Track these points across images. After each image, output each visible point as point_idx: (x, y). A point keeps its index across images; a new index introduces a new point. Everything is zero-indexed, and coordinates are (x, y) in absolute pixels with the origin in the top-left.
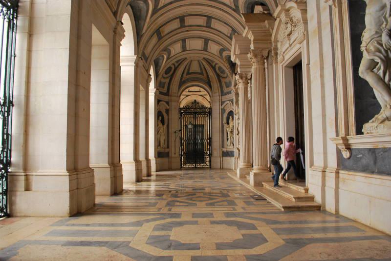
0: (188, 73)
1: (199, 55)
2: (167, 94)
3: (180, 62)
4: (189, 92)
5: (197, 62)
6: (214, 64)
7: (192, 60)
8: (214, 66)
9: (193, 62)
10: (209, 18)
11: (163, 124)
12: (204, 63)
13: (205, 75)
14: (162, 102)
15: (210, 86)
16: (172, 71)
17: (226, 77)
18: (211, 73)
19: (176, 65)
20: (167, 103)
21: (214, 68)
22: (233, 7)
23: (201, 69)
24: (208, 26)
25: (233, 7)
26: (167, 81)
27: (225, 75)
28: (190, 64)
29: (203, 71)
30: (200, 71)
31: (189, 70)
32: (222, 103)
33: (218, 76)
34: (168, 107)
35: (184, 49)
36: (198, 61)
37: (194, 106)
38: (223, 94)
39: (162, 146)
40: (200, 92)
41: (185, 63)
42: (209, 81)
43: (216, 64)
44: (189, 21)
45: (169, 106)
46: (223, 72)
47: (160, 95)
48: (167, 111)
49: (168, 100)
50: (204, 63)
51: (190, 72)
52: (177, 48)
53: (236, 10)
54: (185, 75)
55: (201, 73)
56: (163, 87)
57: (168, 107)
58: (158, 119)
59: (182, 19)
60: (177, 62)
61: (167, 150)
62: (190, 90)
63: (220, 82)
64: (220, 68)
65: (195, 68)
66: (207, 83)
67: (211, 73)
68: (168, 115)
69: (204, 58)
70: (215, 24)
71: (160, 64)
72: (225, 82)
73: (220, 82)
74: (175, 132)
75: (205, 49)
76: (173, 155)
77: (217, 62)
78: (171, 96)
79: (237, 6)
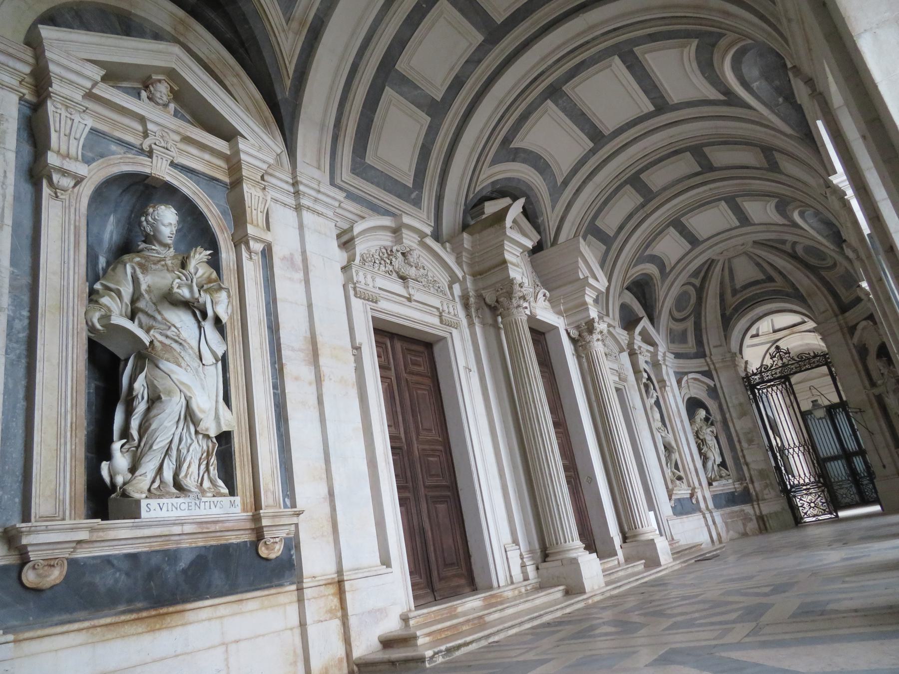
1: (740, 240)
2: (701, 354)
3: (704, 272)
4: (775, 331)
6: (788, 247)
7: (729, 260)
8: (790, 251)
10: (697, 151)
12: (763, 254)
14: (691, 376)
16: (693, 300)
17: (835, 265)
19: (697, 282)
20: (708, 374)
22: (722, 97)
24: (707, 167)
25: (722, 97)
26: (690, 324)
27: (830, 262)
28: (731, 271)
30: (761, 277)
32: (852, 329)
34: (711, 383)
35: (693, 241)
36: (747, 254)
37: (780, 362)
38: (844, 308)
40: (804, 322)
43: (795, 243)
44: (656, 179)
46: (821, 255)
47: (681, 361)
49: (706, 368)
50: (763, 254)
51: (738, 286)
52: (671, 247)
53: (731, 99)
55: (770, 279)
59: (635, 181)
60: (695, 274)
62: (777, 327)
69: (754, 242)
70: (720, 157)
75: (744, 219)
77: (790, 238)
79: (728, 92)
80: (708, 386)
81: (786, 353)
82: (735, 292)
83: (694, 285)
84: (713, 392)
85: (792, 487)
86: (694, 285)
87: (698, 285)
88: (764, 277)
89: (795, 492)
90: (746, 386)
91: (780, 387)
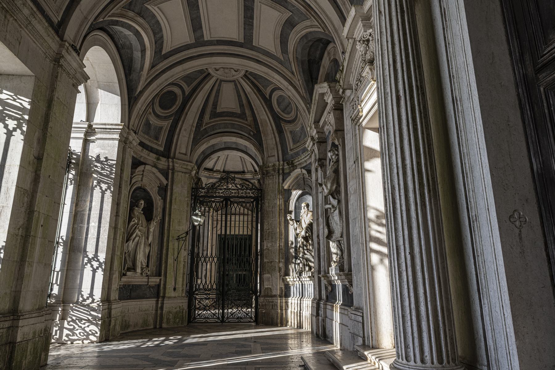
0: (214, 114)
5: (232, 85)
7: (221, 81)
8: (267, 97)
9: (224, 85)
11: (149, 218)
13: (250, 119)
15: (260, 146)
18: (263, 115)
19: (187, 90)
20: (165, 173)
21: (268, 102)
23: (242, 106)
26: (166, 124)
28: (218, 91)
29: (245, 104)
31: (215, 105)
33: (277, 119)
34: (165, 182)
36: (236, 85)
39: (139, 270)
41: (208, 87)
42: (259, 131)
45: (167, 179)
48: (163, 190)
54: (207, 117)
56: (157, 138)
57: (165, 182)
58: (133, 205)
60: (188, 79)
61: (154, 280)
63: (280, 131)
64: (281, 99)
65: (228, 101)
66: (254, 136)
67: (263, 115)
68: (164, 199)
71: (137, 65)
72: (291, 132)
73: (280, 131)
74: (178, 239)
76: (170, 292)
78: (174, 158)
80: (161, 183)
81: (232, 180)
82: (214, 114)
83: (183, 91)
84: (163, 190)
85: (196, 290)
86: (183, 91)
87: (187, 93)
88: (239, 112)
89: (197, 294)
90: (192, 195)
91: (218, 204)
